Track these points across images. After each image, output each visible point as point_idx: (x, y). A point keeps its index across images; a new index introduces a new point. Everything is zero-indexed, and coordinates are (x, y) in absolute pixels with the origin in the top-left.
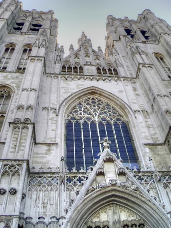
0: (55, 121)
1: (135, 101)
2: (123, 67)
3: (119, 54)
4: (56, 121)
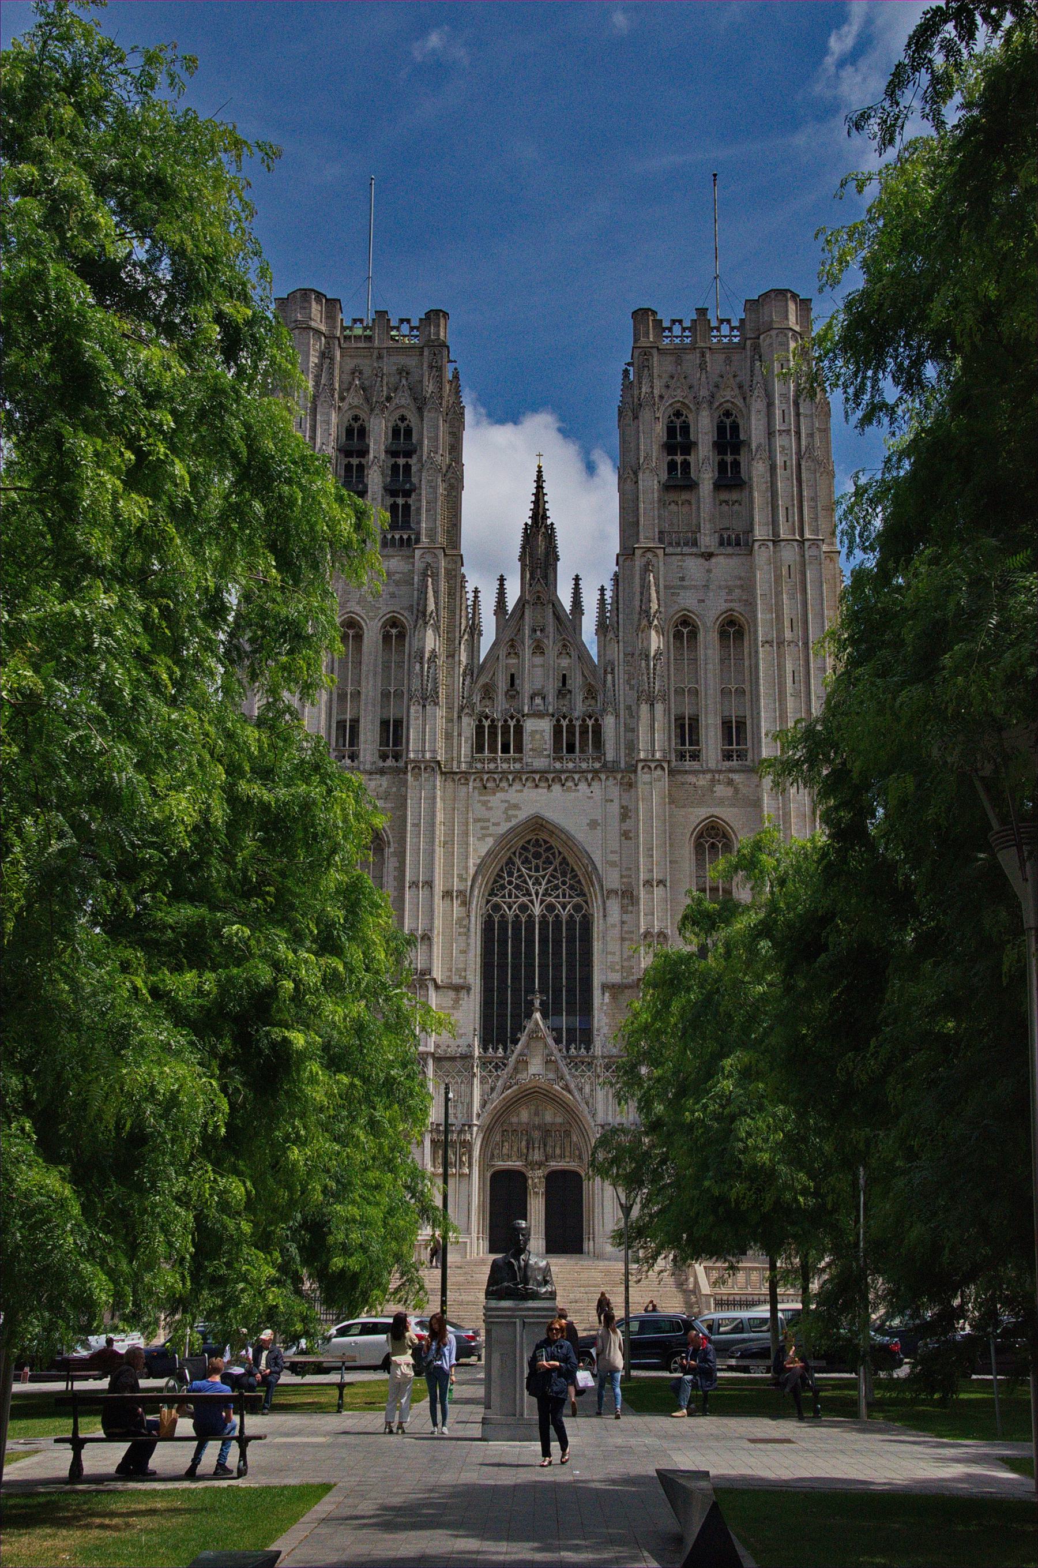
0: (465, 926)
1: (617, 859)
2: (617, 716)
3: (621, 644)
4: (469, 930)
